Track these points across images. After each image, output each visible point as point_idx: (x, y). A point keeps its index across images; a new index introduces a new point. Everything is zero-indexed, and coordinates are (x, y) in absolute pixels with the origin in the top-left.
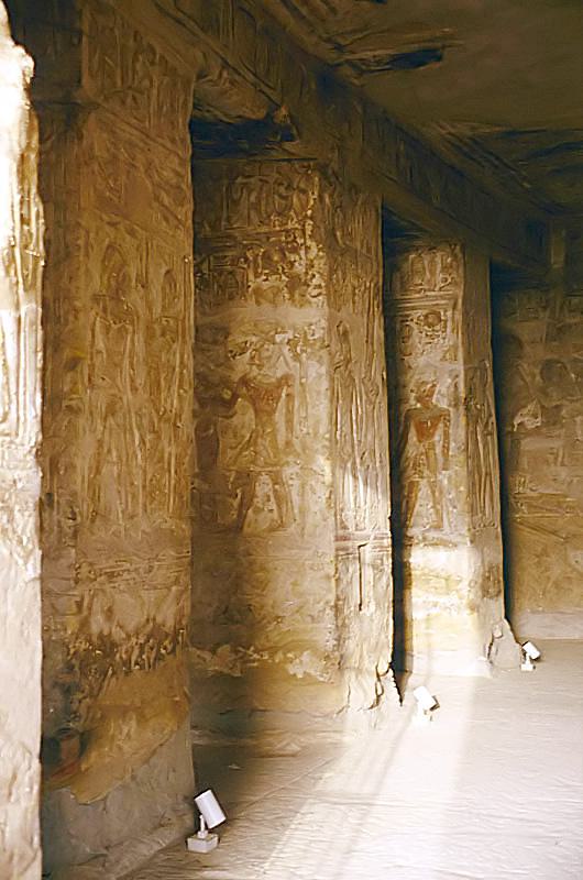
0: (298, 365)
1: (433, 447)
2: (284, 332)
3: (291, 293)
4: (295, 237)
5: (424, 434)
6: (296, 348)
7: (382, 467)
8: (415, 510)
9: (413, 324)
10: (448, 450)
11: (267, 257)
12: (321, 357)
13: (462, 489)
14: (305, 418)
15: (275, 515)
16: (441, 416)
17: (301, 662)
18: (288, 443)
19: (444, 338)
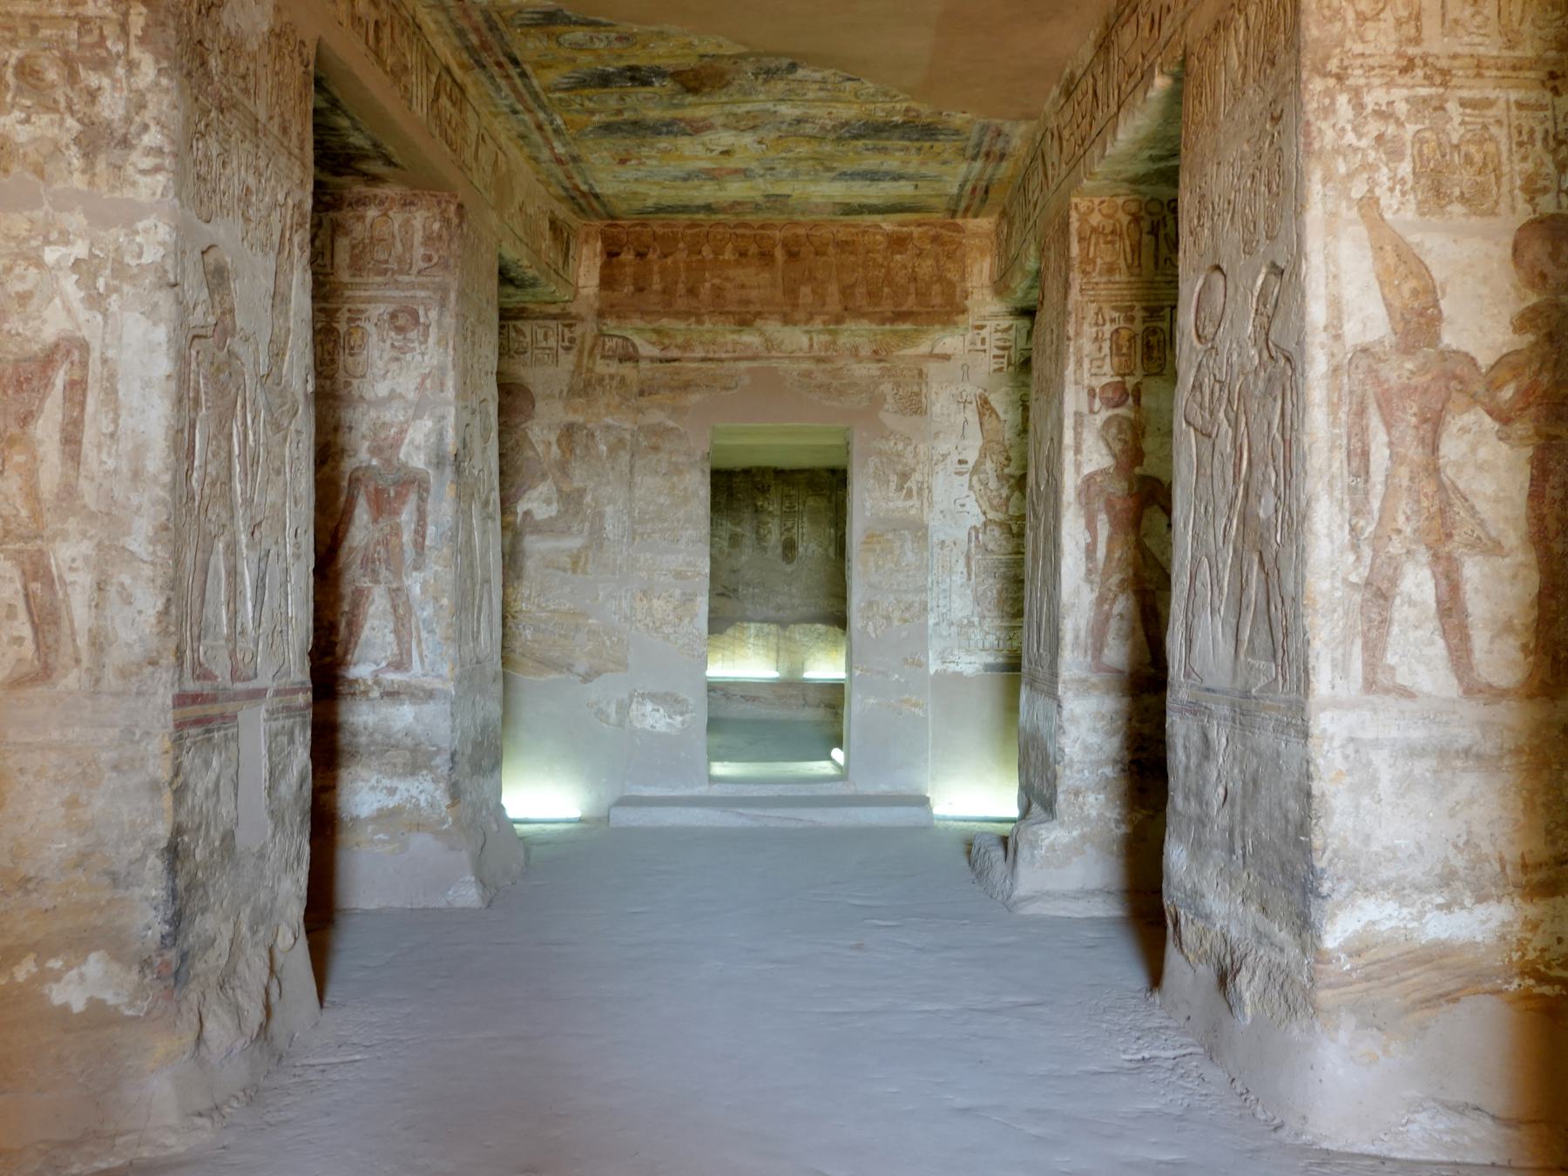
0: (99, 318)
1: (397, 531)
2: (67, 243)
3: (89, 155)
4: (103, 38)
5: (382, 506)
6: (95, 276)
7: (297, 557)
8: (363, 637)
9: (370, 327)
10: (424, 537)
11: (26, 71)
12: (155, 305)
13: (445, 601)
14: (112, 435)
15: (29, 649)
16: (412, 482)
17: (82, 977)
18: (68, 492)
19: (423, 354)
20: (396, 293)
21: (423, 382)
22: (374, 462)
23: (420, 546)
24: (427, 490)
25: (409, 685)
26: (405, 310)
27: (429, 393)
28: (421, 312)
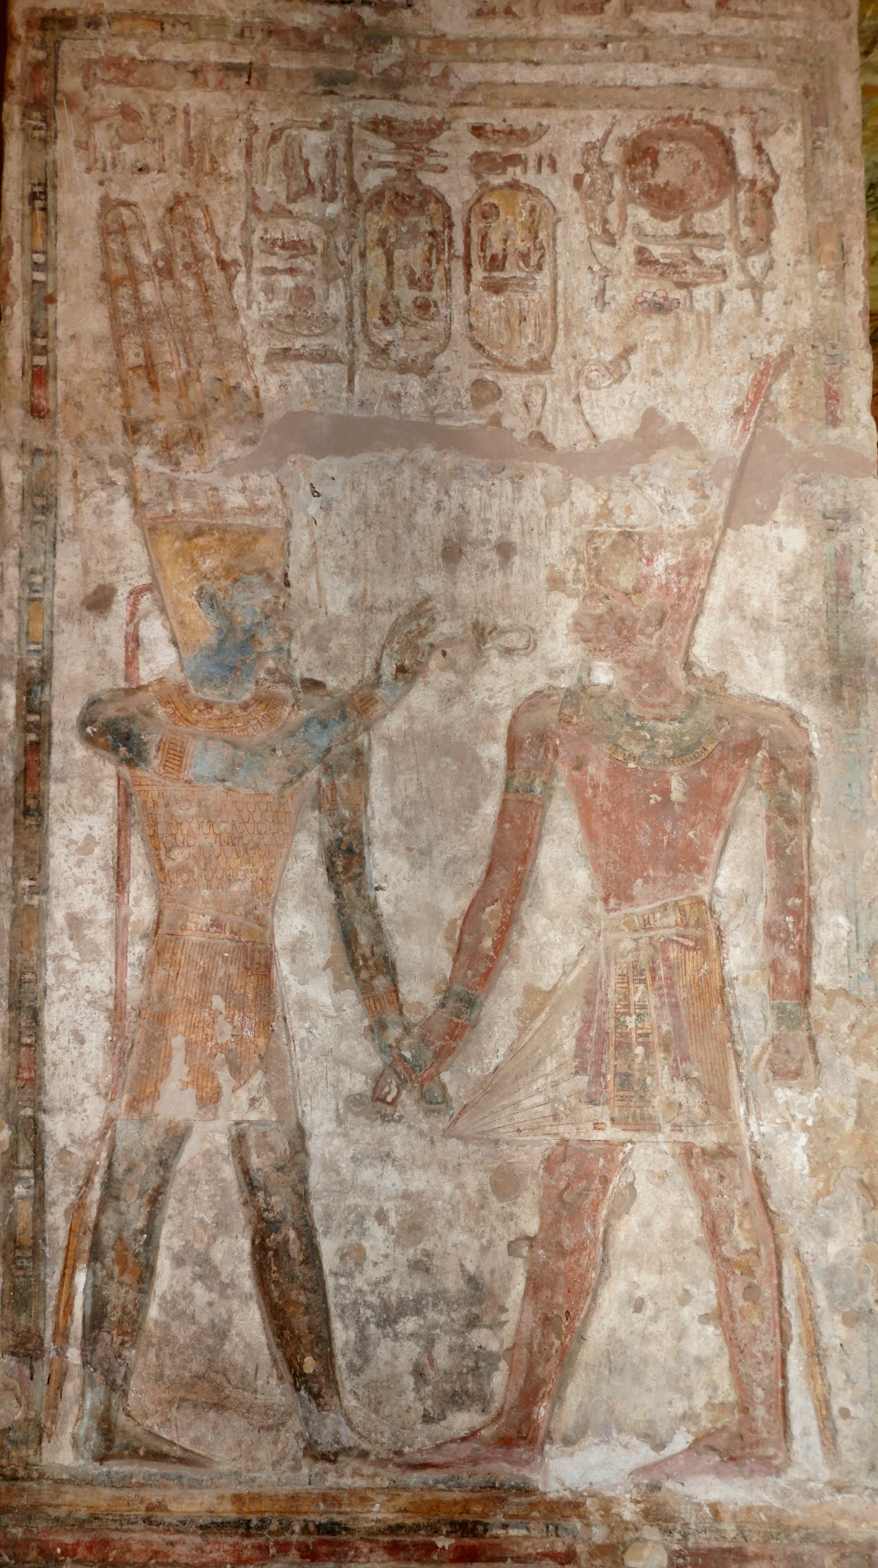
1: (703, 933)
9: (556, 189)
20: (646, 75)
21: (760, 391)
22: (603, 674)
23: (795, 990)
24: (805, 781)
25: (779, 1526)
26: (678, 128)
27: (785, 429)
28: (741, 141)
